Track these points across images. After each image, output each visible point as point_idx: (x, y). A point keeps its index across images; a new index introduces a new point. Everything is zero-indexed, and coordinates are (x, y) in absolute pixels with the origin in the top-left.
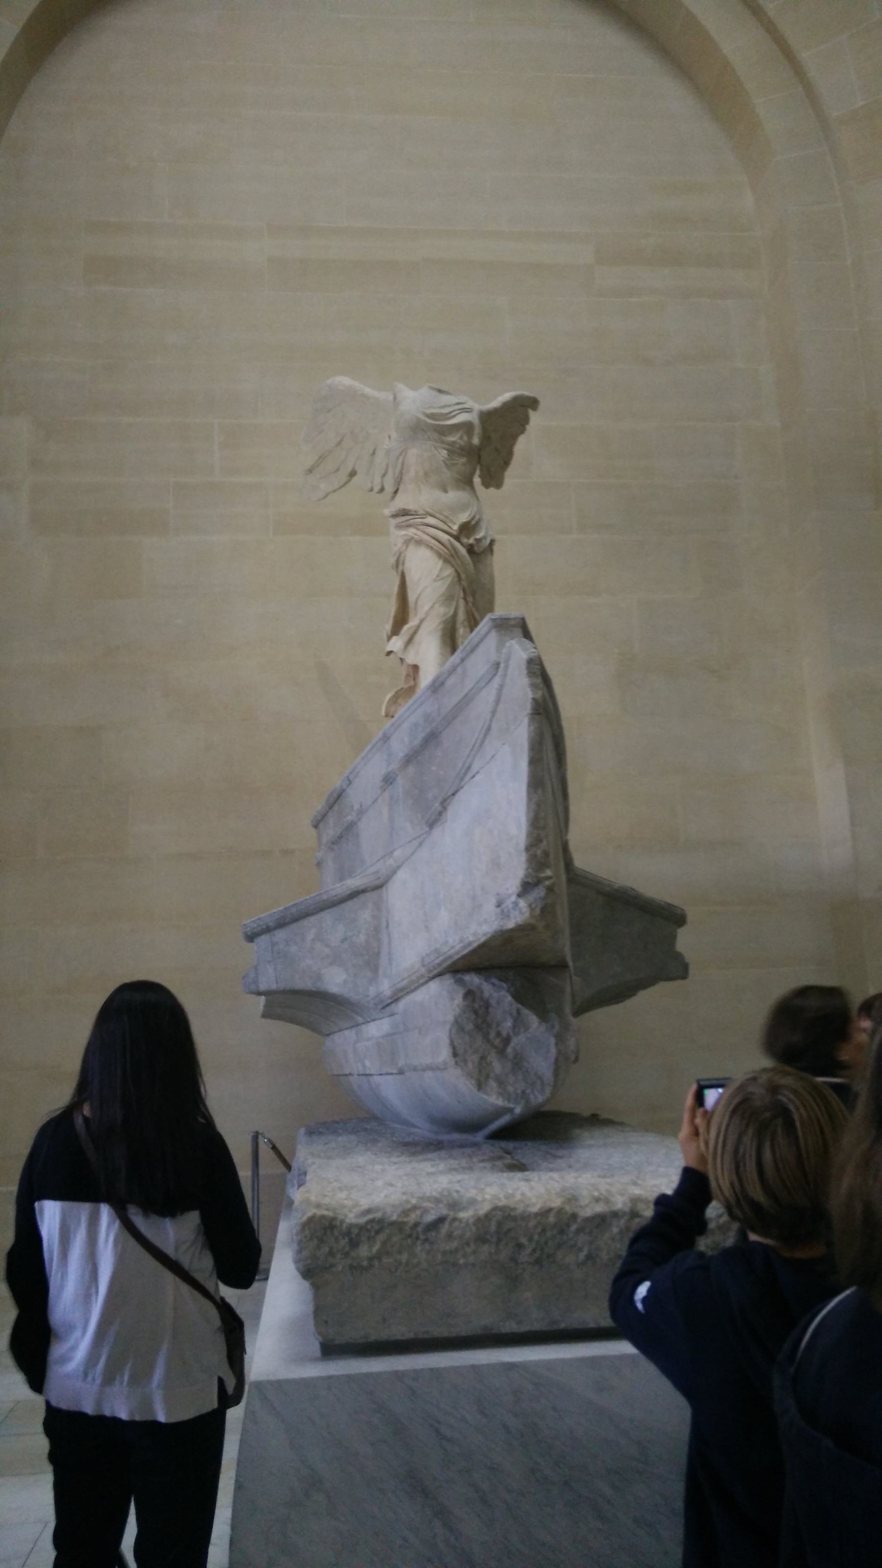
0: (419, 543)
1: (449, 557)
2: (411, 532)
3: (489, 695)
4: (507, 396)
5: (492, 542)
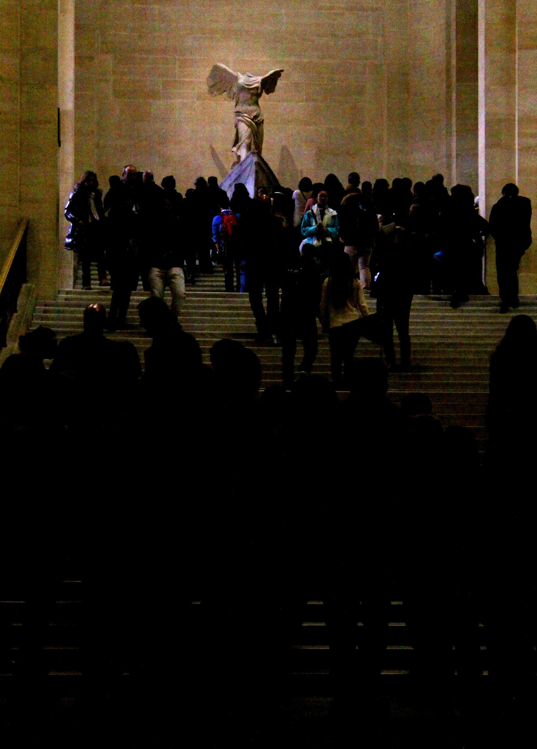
0: (242, 121)
1: (250, 126)
2: (240, 118)
3: (250, 168)
4: (272, 72)
5: (263, 120)
